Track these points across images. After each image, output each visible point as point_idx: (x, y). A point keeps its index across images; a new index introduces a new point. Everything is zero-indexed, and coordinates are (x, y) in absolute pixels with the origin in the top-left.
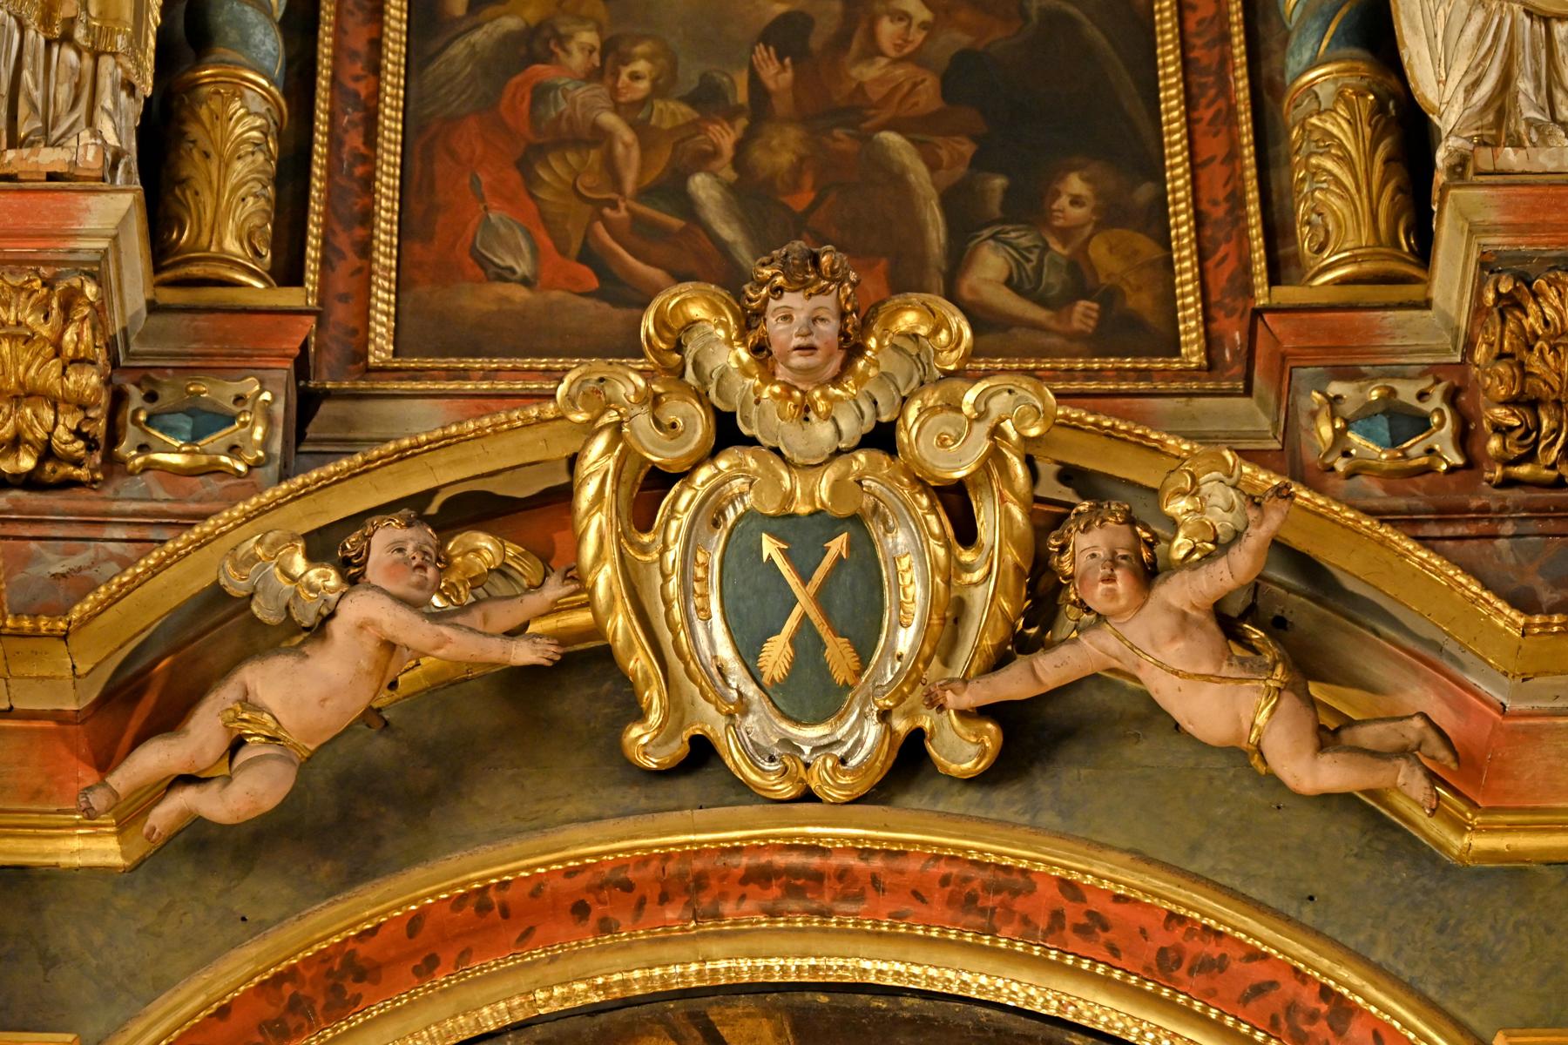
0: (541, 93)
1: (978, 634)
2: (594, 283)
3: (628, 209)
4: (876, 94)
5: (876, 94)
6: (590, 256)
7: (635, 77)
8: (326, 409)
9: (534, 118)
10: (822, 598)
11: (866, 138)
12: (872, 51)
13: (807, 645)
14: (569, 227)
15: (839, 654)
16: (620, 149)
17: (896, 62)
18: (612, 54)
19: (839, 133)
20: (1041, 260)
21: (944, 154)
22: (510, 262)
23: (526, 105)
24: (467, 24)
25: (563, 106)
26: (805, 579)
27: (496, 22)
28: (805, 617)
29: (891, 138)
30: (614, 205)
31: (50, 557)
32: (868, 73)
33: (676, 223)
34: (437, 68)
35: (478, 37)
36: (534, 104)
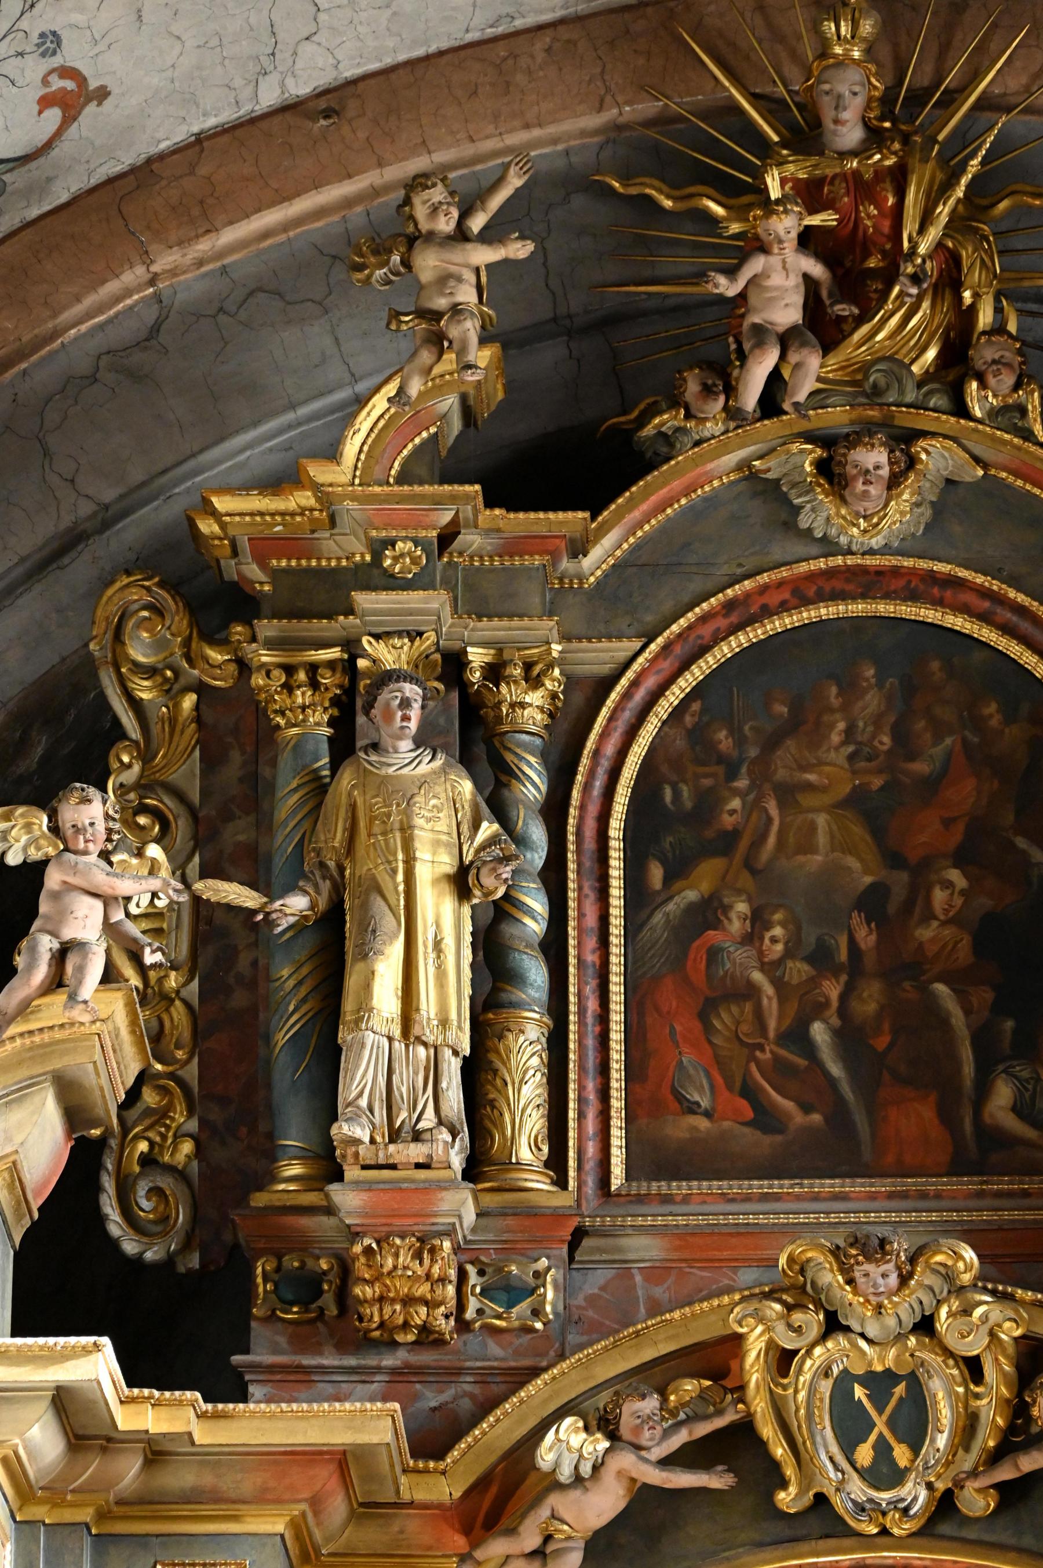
0: (714, 954)
1: (987, 1439)
2: (749, 1114)
3: (772, 1052)
4: (931, 950)
5: (931, 950)
6: (749, 1092)
7: (774, 940)
8: (587, 1243)
9: (709, 977)
10: (891, 1424)
11: (924, 989)
12: (929, 916)
13: (882, 1449)
14: (734, 1067)
15: (901, 1454)
16: (765, 1001)
17: (944, 924)
19: (907, 985)
20: (1035, 1090)
21: (974, 1000)
22: (697, 1098)
23: (703, 965)
24: (663, 897)
25: (728, 965)
26: (880, 1411)
27: (683, 894)
28: (881, 1435)
29: (941, 988)
30: (762, 1050)
31: (429, 1394)
33: (802, 1062)
34: (645, 934)
35: (671, 907)
36: (708, 966)
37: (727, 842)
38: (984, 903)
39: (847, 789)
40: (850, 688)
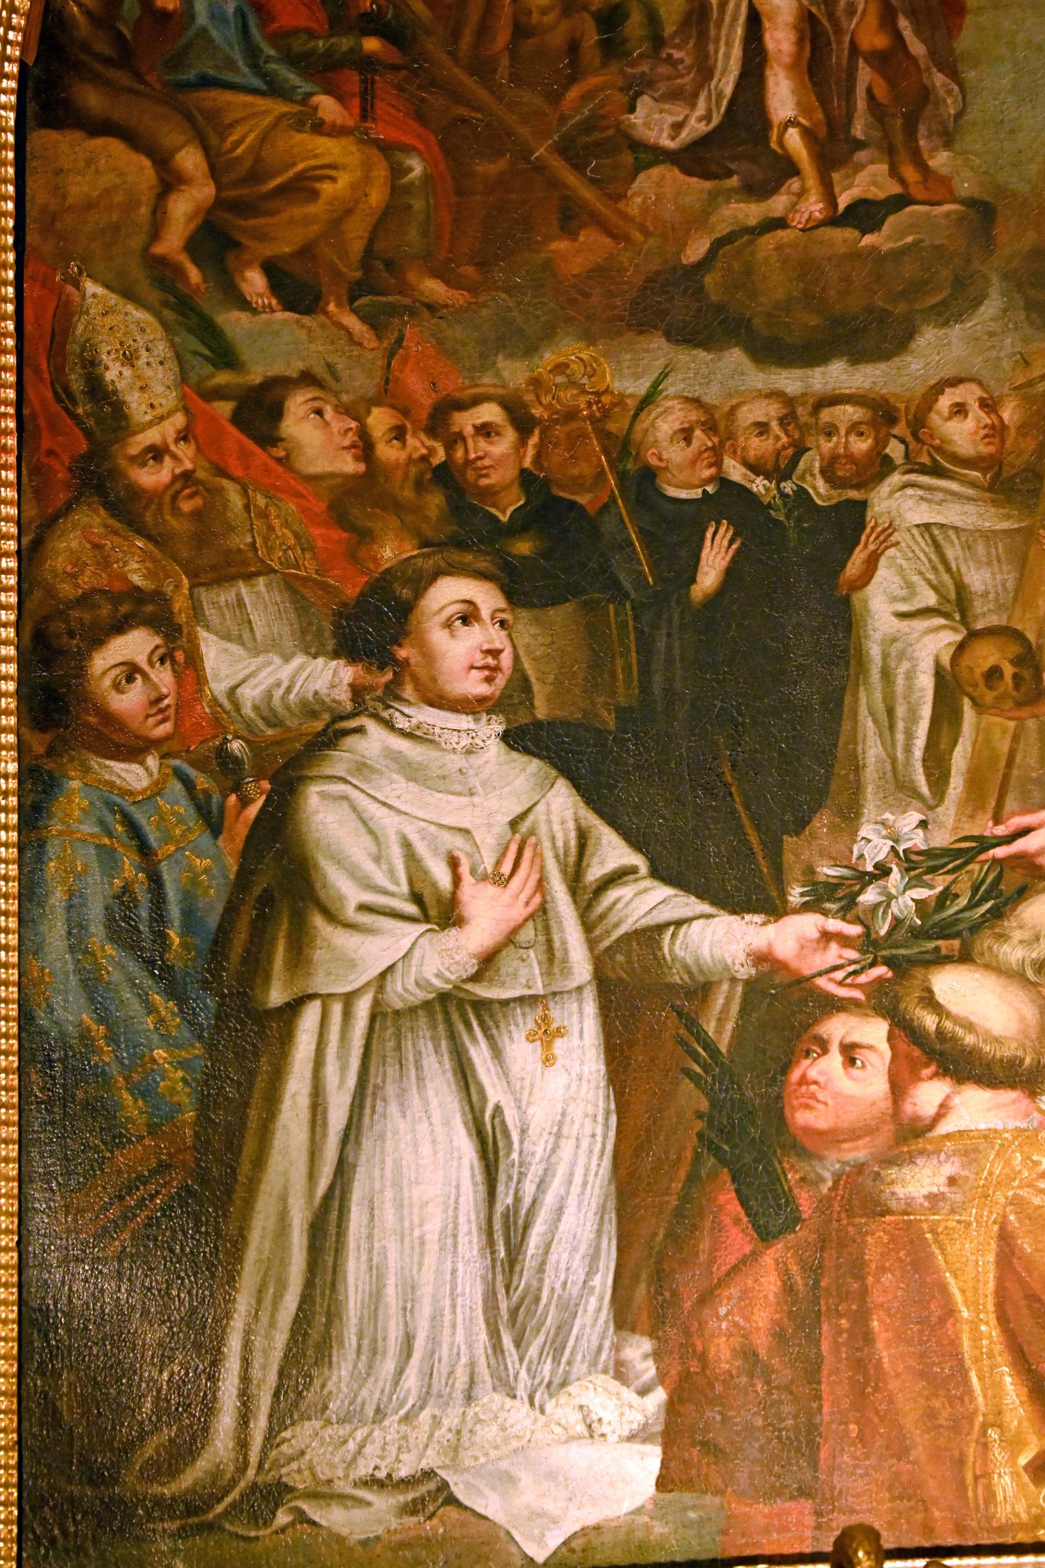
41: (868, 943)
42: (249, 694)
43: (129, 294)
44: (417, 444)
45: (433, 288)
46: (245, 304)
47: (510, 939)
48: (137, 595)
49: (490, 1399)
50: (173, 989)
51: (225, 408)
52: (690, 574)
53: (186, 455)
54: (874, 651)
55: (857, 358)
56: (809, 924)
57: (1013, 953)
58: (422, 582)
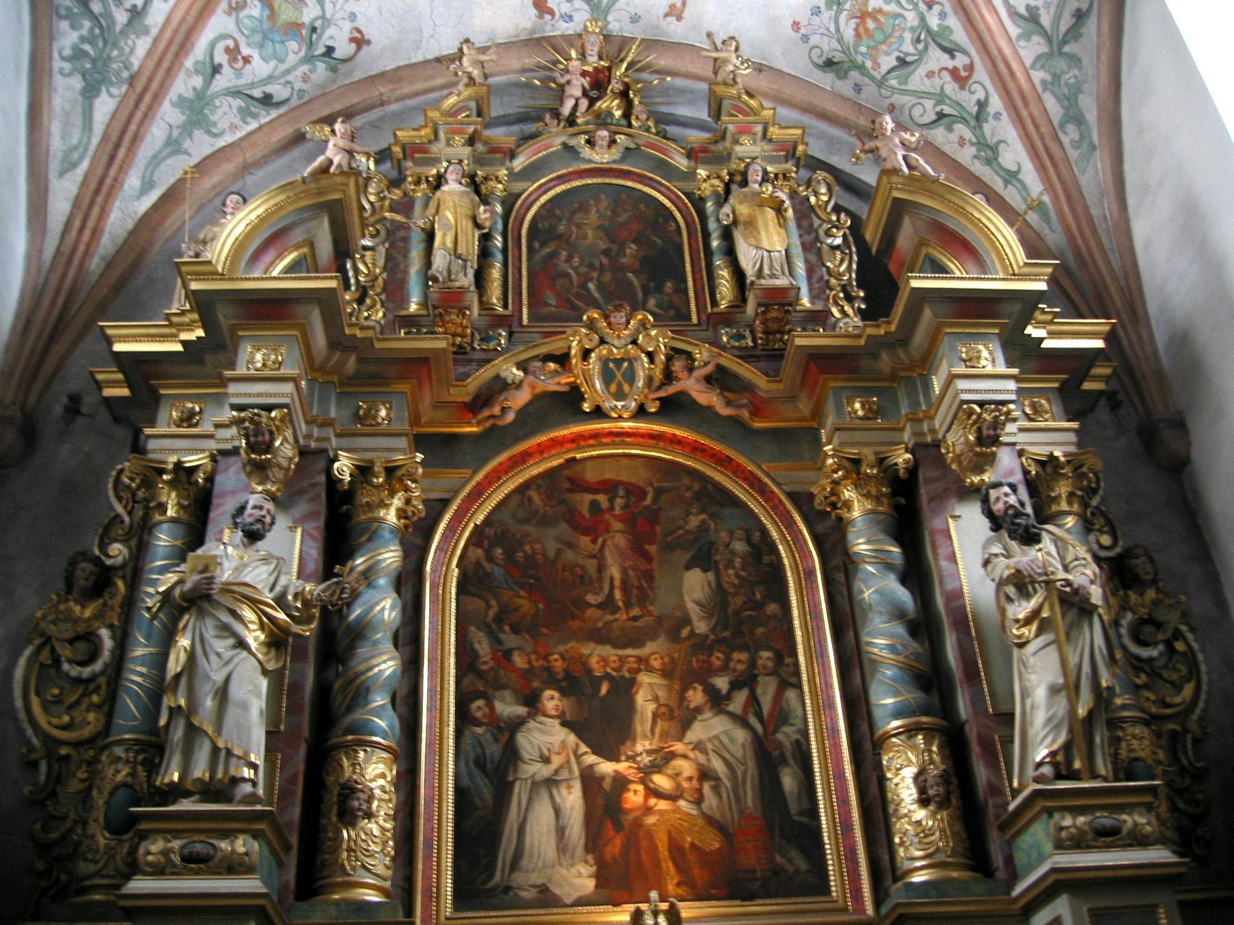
1: (656, 383)
6: (568, 301)
8: (516, 335)
10: (623, 376)
12: (625, 256)
13: (620, 386)
15: (626, 388)
18: (570, 258)
29: (630, 275)
32: (624, 261)
37: (560, 237)
38: (642, 253)
39: (597, 224)
40: (597, 201)
41: (639, 769)
42: (505, 714)
43: (479, 629)
44: (541, 662)
45: (545, 631)
46: (504, 632)
47: (561, 767)
48: (481, 692)
49: (558, 868)
50: (487, 776)
51: (500, 654)
52: (599, 690)
53: (492, 664)
54: (639, 708)
55: (635, 647)
56: (625, 764)
57: (669, 772)
58: (542, 691)
